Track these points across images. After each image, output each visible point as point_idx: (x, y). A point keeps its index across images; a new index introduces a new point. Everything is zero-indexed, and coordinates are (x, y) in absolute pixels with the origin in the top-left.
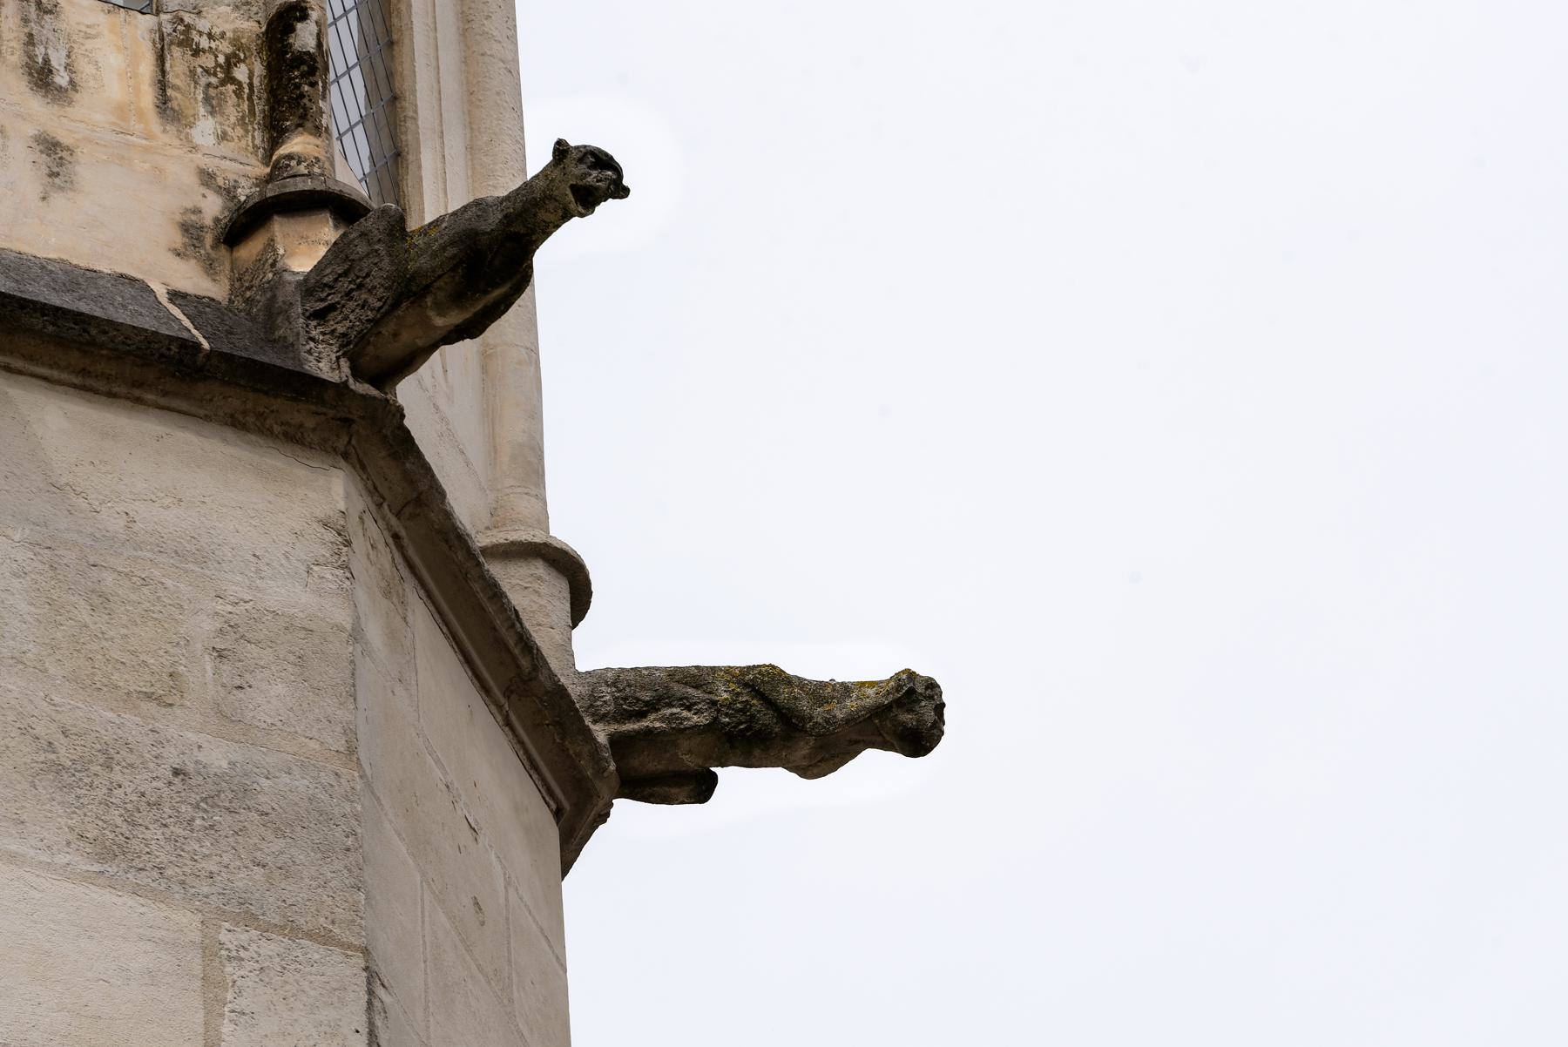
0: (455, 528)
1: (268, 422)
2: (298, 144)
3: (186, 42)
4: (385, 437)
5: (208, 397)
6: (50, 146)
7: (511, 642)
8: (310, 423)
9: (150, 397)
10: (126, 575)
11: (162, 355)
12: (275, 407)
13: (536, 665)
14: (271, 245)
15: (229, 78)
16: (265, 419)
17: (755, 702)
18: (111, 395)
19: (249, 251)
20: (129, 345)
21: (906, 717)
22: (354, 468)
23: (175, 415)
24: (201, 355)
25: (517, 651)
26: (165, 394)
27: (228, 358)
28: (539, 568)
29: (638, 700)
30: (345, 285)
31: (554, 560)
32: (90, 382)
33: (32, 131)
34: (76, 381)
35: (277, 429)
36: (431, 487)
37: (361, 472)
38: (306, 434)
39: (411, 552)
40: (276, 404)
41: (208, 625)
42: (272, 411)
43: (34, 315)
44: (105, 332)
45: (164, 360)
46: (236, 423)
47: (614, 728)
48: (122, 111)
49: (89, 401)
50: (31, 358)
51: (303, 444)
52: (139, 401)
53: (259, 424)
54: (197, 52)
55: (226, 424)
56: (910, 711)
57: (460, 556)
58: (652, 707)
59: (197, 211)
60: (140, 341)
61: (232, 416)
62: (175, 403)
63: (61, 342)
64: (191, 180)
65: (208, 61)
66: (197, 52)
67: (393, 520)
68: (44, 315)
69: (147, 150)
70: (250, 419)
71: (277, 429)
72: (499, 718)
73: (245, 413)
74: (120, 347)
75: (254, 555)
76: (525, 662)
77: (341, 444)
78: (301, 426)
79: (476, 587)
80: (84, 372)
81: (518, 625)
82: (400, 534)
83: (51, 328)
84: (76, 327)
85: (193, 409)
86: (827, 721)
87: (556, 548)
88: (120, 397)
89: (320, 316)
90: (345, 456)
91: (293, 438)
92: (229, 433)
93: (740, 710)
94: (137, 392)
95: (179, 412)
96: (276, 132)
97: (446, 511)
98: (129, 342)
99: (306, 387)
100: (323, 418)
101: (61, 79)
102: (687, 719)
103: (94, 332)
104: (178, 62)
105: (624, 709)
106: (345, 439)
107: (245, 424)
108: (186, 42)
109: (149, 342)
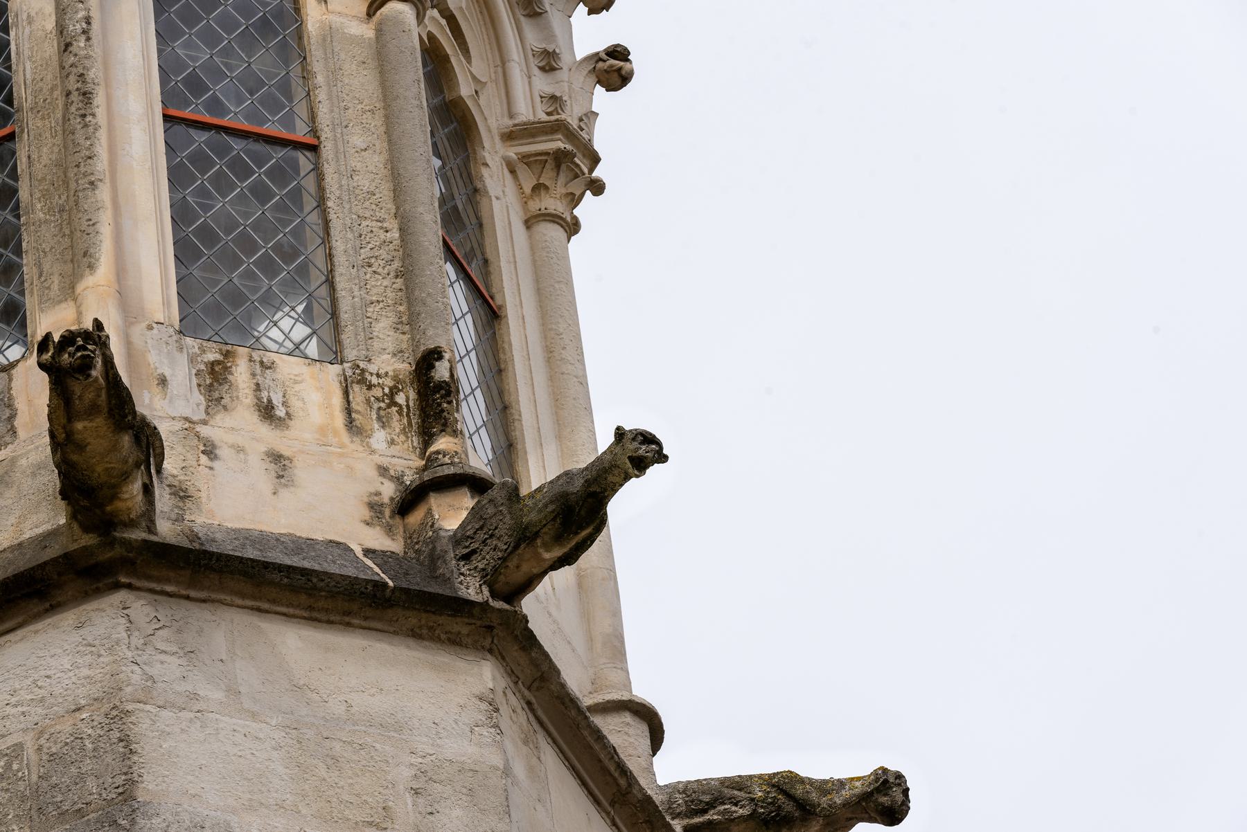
0: (568, 695)
1: (437, 632)
2: (443, 443)
3: (362, 381)
4: (517, 636)
5: (395, 619)
6: (276, 458)
7: (612, 768)
8: (465, 630)
9: (356, 621)
10: (349, 743)
11: (362, 593)
12: (440, 622)
13: (630, 783)
14: (429, 512)
15: (393, 403)
16: (435, 631)
17: (780, 796)
18: (330, 622)
19: (415, 518)
20: (339, 588)
21: (884, 800)
22: (497, 658)
23: (374, 633)
24: (388, 590)
25: (616, 775)
26: (366, 618)
27: (406, 591)
28: (627, 717)
29: (701, 801)
30: (481, 536)
31: (637, 711)
32: (315, 614)
33: (263, 449)
34: (305, 615)
35: (443, 636)
36: (550, 668)
37: (501, 661)
38: (462, 638)
39: (540, 712)
40: (442, 619)
41: (407, 773)
42: (439, 625)
43: (275, 572)
44: (323, 580)
45: (363, 596)
46: (415, 635)
47: (686, 822)
48: (322, 430)
49: (315, 627)
50: (273, 601)
51: (461, 645)
52: (348, 624)
53: (430, 634)
54: (370, 387)
55: (408, 636)
56: (886, 795)
57: (573, 713)
58: (711, 805)
59: (378, 494)
60: (346, 585)
61: (412, 630)
62: (373, 624)
63: (294, 589)
64: (373, 473)
65: (378, 392)
66: (370, 387)
67: (526, 693)
68: (280, 572)
69: (341, 455)
70: (425, 631)
71: (443, 636)
72: (608, 821)
73: (420, 627)
74: (334, 589)
75: (434, 723)
76: (623, 782)
77: (487, 643)
78: (459, 633)
79: (586, 733)
80: (311, 608)
81: (616, 757)
82: (532, 702)
83: (286, 580)
84: (303, 578)
85: (386, 628)
86: (830, 806)
87: (638, 703)
88: (336, 623)
89: (466, 558)
90: (490, 651)
91: (454, 642)
92: (411, 642)
93: (771, 803)
94: (347, 619)
95: (376, 630)
96: (427, 437)
97: (561, 683)
98: (339, 585)
99: (461, 606)
100: (473, 627)
101: (280, 412)
102: (735, 812)
103: (315, 580)
104: (358, 394)
105: (693, 809)
106: (490, 640)
107: (421, 635)
108: (362, 381)
109: (353, 585)
